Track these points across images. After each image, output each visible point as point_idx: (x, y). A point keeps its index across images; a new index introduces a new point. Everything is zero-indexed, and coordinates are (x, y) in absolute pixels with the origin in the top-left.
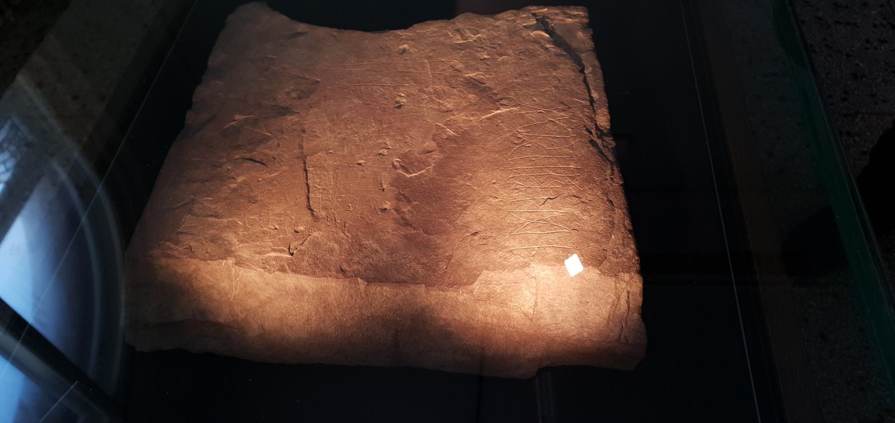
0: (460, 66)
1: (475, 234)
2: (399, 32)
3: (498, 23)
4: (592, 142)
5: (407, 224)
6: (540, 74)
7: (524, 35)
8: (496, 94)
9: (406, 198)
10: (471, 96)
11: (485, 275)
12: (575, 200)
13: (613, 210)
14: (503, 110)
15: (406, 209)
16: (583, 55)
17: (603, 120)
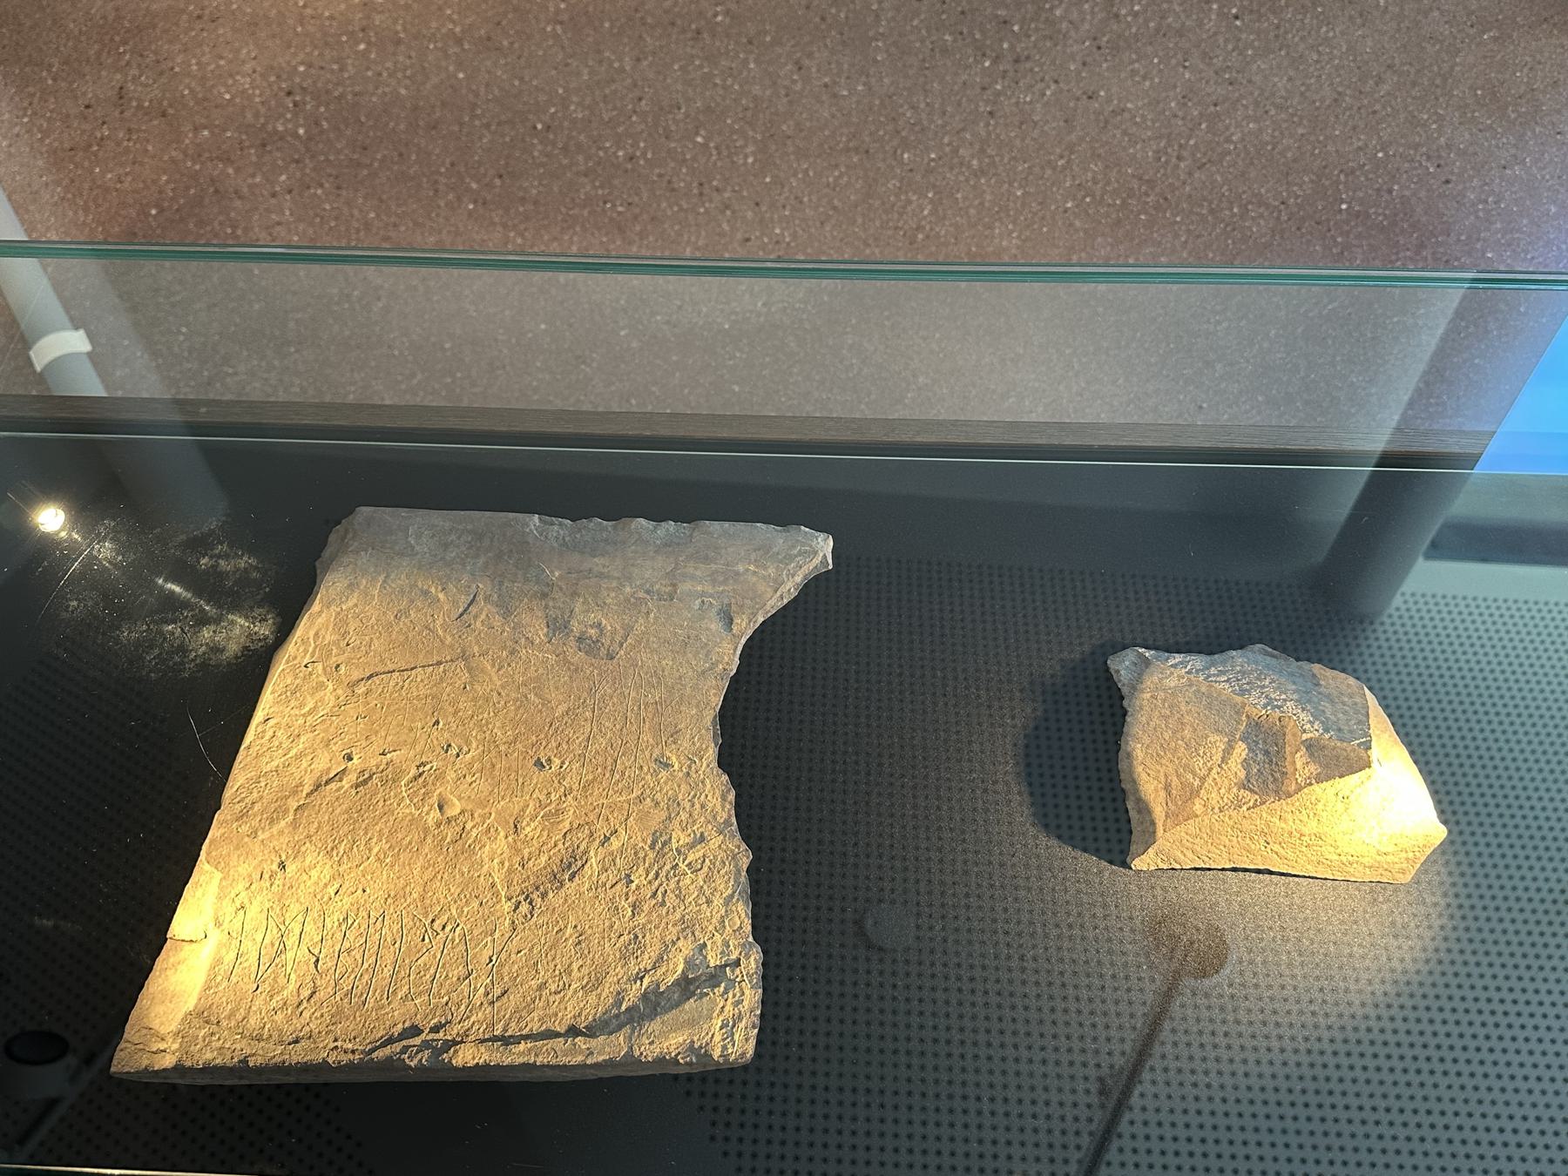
0: (615, 844)
1: (282, 866)
2: (712, 753)
3: (718, 901)
4: (415, 1031)
5: (318, 787)
6: (575, 967)
7: (680, 943)
8: (544, 895)
9: (365, 782)
10: (544, 859)
11: (218, 875)
12: (306, 993)
13: (281, 1042)
14: (507, 906)
15: (346, 783)
16: (621, 1038)
17: (467, 1056)
